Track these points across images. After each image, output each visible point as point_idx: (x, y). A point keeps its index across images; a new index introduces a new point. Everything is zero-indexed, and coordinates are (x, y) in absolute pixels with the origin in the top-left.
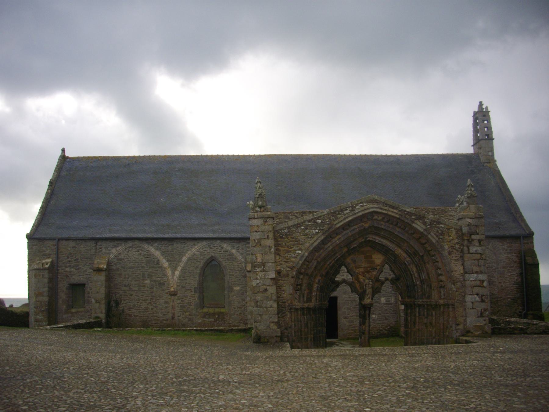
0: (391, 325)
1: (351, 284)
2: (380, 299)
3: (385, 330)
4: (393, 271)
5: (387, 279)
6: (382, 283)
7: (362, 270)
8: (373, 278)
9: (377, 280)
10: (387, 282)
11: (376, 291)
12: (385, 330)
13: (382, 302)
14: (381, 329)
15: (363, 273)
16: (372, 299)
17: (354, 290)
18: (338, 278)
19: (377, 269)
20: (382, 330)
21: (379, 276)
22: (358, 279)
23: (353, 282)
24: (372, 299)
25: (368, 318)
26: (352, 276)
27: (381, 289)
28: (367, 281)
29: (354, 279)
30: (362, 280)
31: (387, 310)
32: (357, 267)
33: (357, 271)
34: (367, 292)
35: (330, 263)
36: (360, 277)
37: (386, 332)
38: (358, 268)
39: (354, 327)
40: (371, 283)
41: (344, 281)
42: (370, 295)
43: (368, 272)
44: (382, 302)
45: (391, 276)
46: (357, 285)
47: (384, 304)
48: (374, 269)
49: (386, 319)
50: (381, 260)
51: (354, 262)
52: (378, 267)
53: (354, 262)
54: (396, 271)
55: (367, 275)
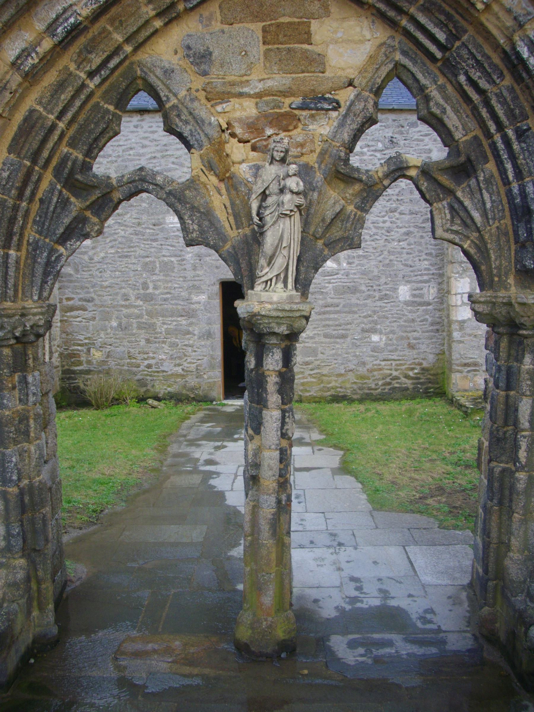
0: (425, 365)
1: (176, 198)
2: (395, 290)
3: (407, 377)
4: (436, 123)
5: (397, 170)
6: (370, 191)
7: (248, 109)
8: (312, 159)
9: (343, 174)
10: (403, 183)
11: (326, 237)
12: (407, 377)
13: (401, 298)
14: (395, 373)
15: (254, 127)
16: (303, 285)
17: (200, 232)
18: (110, 164)
19: (337, 106)
20: (396, 378)
21: (350, 148)
22: (218, 165)
23: (193, 183)
24: (303, 285)
25: (273, 398)
26: (189, 146)
27: (360, 222)
28: (271, 171)
29: (197, 163)
30: (243, 171)
31: (413, 321)
32: (216, 97)
33: (216, 116)
34: (270, 240)
35: (25, 53)
36: (236, 151)
37: (408, 383)
38: (224, 97)
39: (319, 367)
40: (294, 183)
41: (140, 183)
42: (286, 259)
43: (285, 121)
44: (401, 298)
45: (426, 147)
46: (219, 202)
47: (407, 303)
48: (317, 102)
49: (411, 347)
50: (368, 48)
51: (201, 59)
52: (346, 96)
53: (201, 59)
54: (452, 120)
55: (281, 141)
